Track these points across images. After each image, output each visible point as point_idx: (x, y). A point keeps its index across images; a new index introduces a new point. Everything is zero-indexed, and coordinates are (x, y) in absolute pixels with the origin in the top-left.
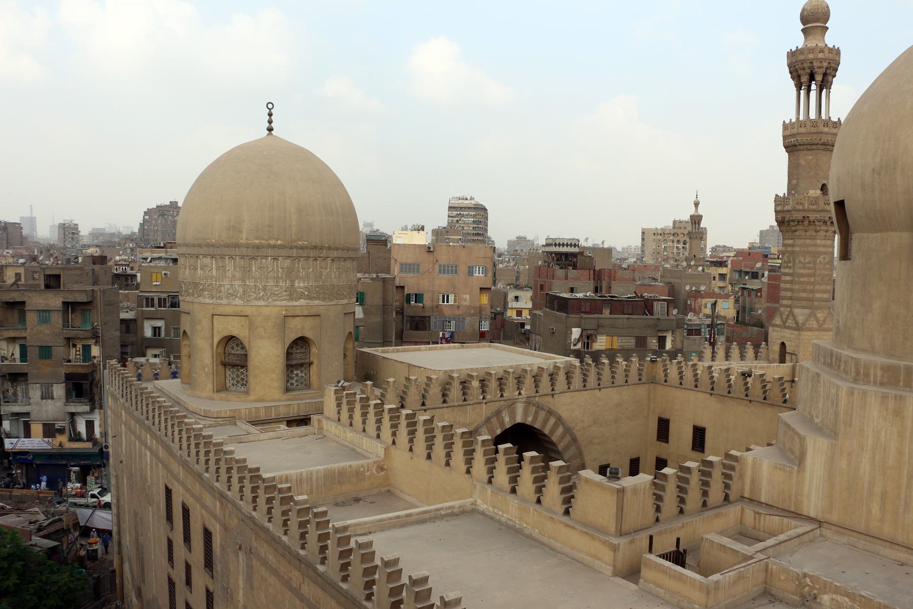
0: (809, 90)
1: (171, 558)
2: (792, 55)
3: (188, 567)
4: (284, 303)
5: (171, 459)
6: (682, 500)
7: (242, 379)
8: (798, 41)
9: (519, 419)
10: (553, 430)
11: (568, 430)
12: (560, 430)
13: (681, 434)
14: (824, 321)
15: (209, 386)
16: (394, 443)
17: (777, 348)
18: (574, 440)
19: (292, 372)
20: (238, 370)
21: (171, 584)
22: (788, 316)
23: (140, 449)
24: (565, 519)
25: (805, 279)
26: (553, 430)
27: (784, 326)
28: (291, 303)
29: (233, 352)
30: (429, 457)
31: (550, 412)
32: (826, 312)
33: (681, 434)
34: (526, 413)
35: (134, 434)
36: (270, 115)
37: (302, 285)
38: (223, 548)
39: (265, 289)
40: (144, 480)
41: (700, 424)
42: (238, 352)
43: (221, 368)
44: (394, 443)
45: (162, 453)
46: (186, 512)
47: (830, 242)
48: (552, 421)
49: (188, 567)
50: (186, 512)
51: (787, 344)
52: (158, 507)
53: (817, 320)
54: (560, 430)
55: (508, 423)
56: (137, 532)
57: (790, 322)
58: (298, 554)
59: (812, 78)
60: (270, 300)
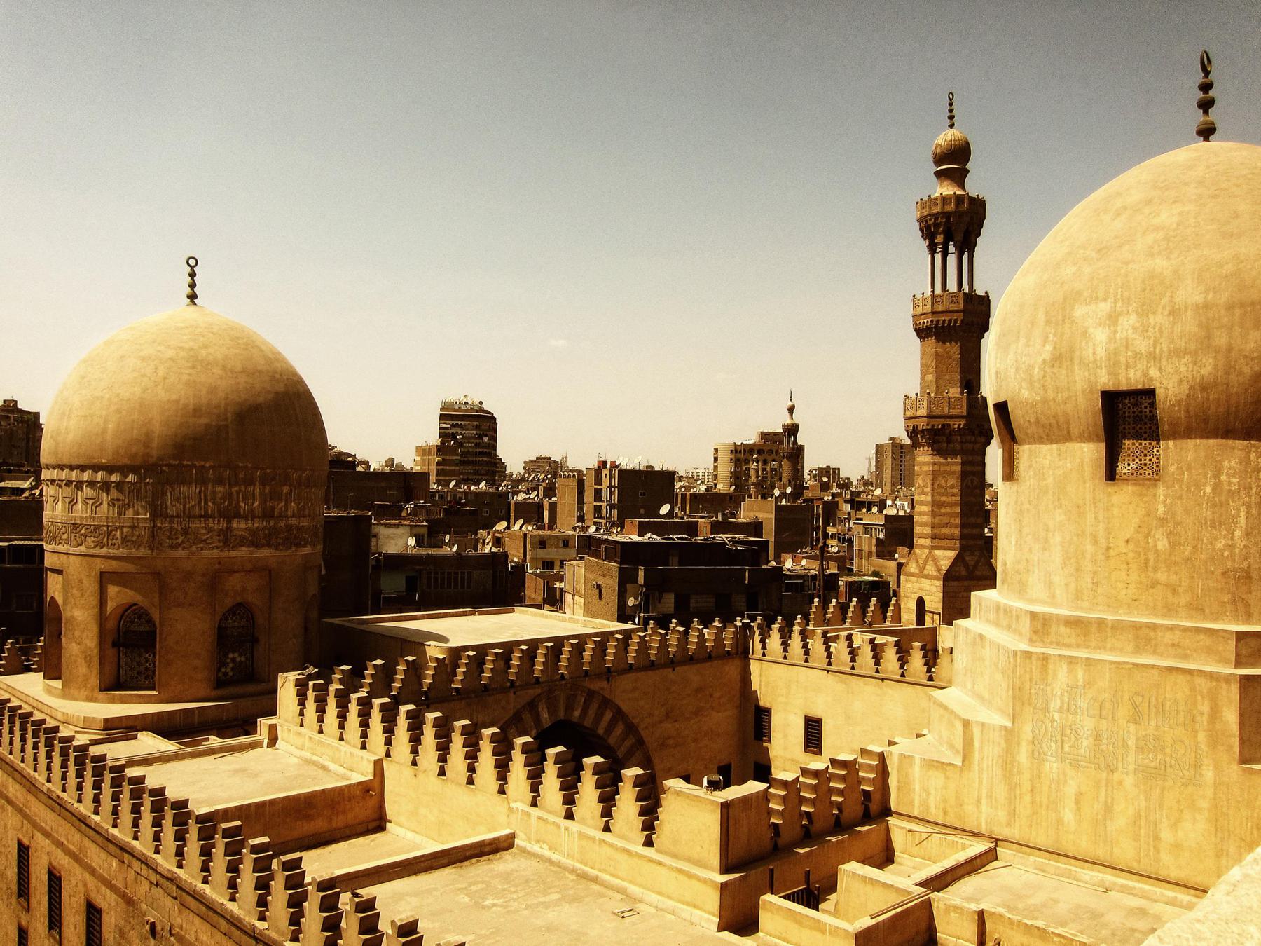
0: (945, 255)
4: (215, 554)
5: (30, 797)
7: (147, 669)
11: (631, 729)
12: (619, 729)
14: (975, 567)
15: (94, 680)
16: (388, 755)
17: (912, 605)
19: (226, 656)
20: (140, 656)
22: (926, 560)
24: (648, 851)
25: (948, 510)
26: (609, 730)
27: (921, 574)
28: (225, 555)
29: (132, 628)
30: (442, 773)
31: (606, 703)
32: (977, 553)
36: (193, 275)
37: (243, 526)
39: (185, 532)
41: (816, 712)
42: (142, 629)
43: (111, 652)
44: (388, 755)
46: (55, 881)
47: (979, 458)
48: (608, 716)
50: (55, 881)
51: (926, 598)
53: (966, 566)
58: (254, 928)
60: (194, 548)
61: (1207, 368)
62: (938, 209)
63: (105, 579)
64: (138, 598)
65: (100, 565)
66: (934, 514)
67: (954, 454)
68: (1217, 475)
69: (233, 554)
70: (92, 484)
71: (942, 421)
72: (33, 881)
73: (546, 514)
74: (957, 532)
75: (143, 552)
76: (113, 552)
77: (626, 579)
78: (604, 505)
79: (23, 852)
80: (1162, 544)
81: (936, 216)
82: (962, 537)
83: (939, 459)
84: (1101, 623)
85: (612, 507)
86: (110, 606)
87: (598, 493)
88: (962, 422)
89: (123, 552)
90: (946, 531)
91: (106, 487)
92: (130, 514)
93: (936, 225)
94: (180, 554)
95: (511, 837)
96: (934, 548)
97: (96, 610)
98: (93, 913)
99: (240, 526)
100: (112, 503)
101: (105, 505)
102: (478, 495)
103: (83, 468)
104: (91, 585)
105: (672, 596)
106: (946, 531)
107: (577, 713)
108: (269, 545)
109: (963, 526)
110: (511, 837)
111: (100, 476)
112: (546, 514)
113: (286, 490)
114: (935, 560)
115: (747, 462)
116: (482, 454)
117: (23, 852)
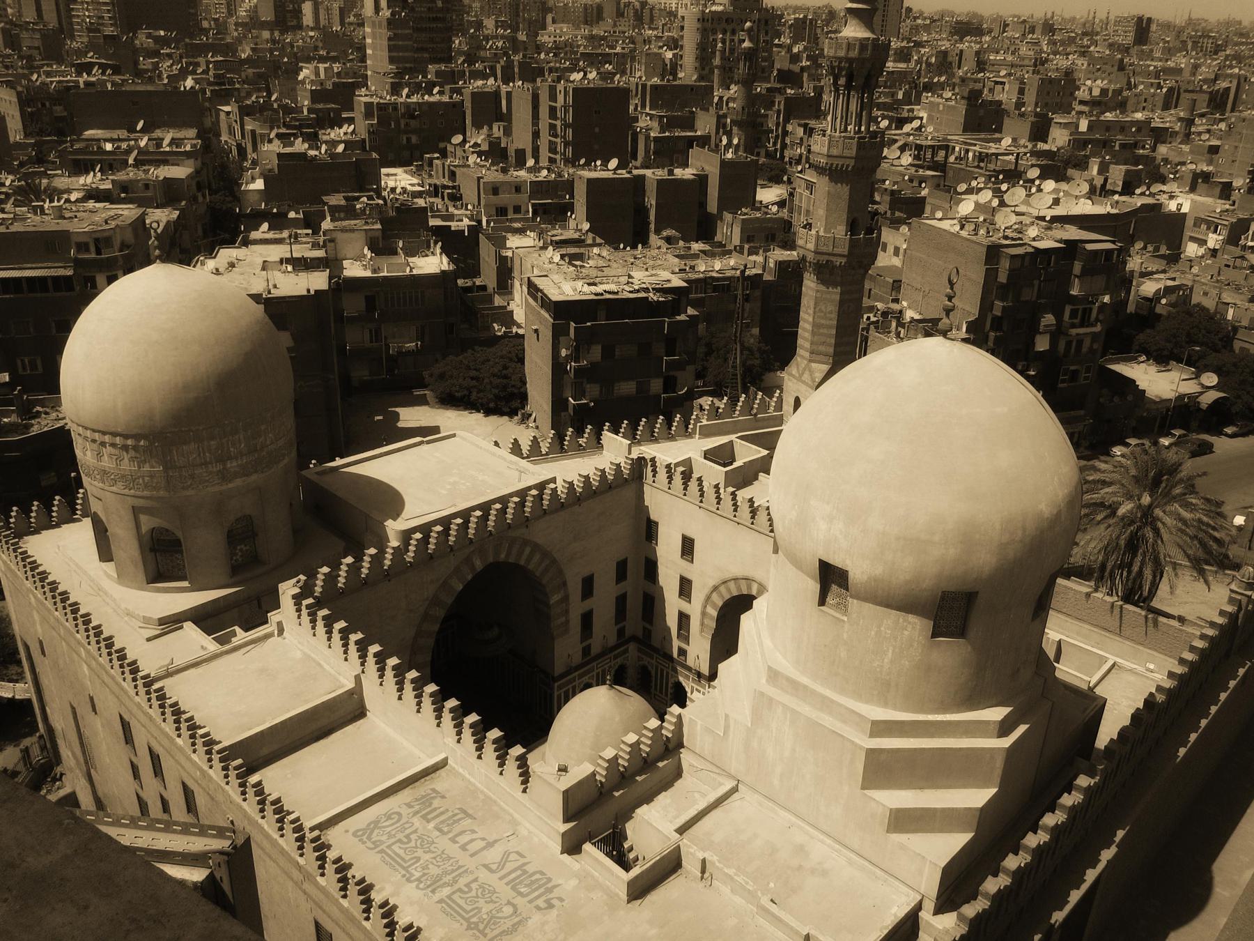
4: (217, 488)
9: (491, 560)
11: (546, 554)
12: (537, 557)
15: (141, 576)
18: (554, 561)
27: (799, 379)
28: (224, 487)
31: (526, 543)
37: (235, 464)
39: (192, 477)
48: (528, 550)
54: (537, 557)
55: (479, 564)
57: (806, 377)
61: (879, 570)
62: (842, 53)
63: (136, 511)
64: (165, 525)
65: (131, 501)
66: (813, 333)
67: (835, 285)
68: (879, 627)
69: (230, 485)
70: (113, 445)
71: (826, 257)
73: (504, 103)
74: (831, 350)
75: (162, 493)
76: (138, 493)
77: (558, 333)
78: (558, 123)
80: (843, 654)
81: (840, 59)
82: (836, 354)
83: (823, 288)
84: (805, 687)
85: (566, 126)
86: (144, 529)
87: (553, 111)
88: (844, 260)
89: (146, 493)
90: (822, 348)
91: (125, 448)
92: (147, 468)
93: (840, 69)
94: (190, 492)
95: (446, 759)
96: (810, 361)
97: (135, 531)
99: (232, 465)
100: (132, 459)
101: (126, 460)
102: (431, 105)
103: (104, 433)
104: (128, 517)
105: (599, 347)
106: (822, 348)
107: (503, 556)
108: (256, 472)
109: (836, 345)
110: (446, 759)
111: (118, 440)
112: (504, 103)
113: (263, 427)
114: (811, 372)
115: (714, 32)
116: (435, 19)
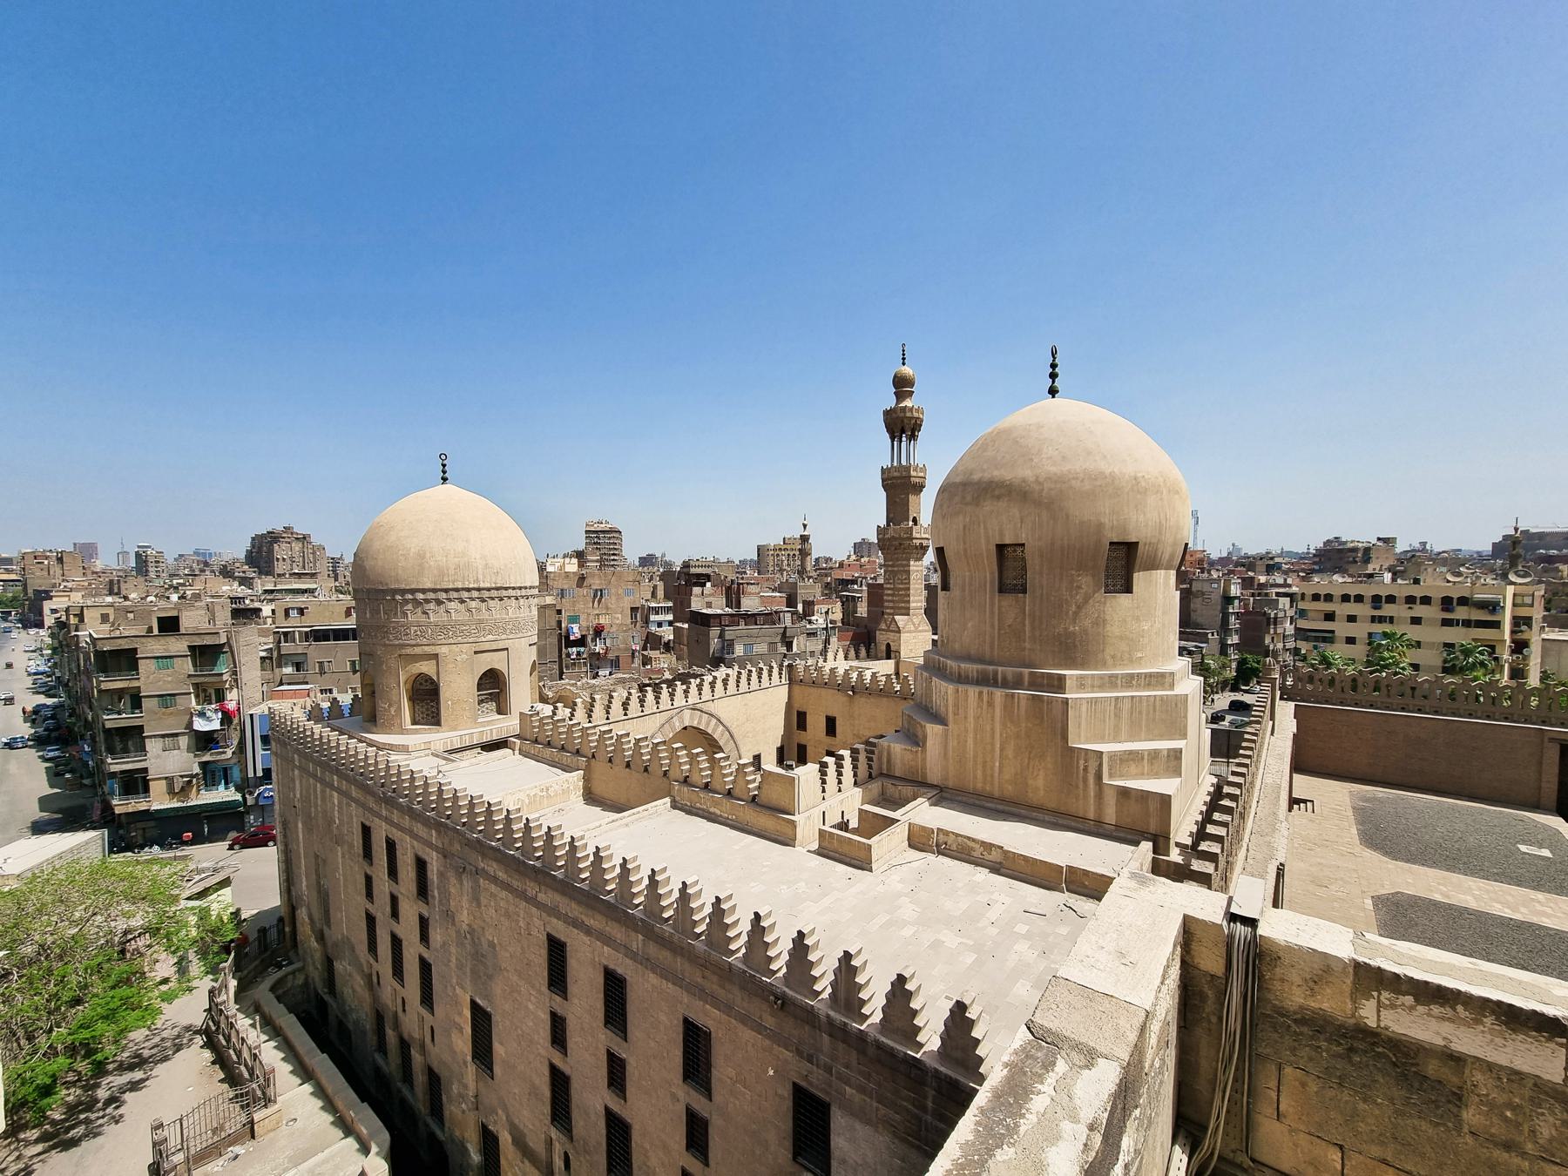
1: (369, 894)
2: (887, 413)
3: (394, 900)
6: (840, 782)
8: (891, 402)
10: (714, 730)
13: (816, 724)
21: (371, 920)
23: (323, 792)
26: (714, 730)
33: (816, 724)
34: (692, 718)
35: (315, 776)
38: (441, 875)
40: (330, 822)
45: (354, 792)
46: (391, 846)
49: (394, 900)
50: (391, 846)
52: (351, 846)
56: (318, 875)
57: (893, 627)
59: (903, 431)
72: (374, 847)
79: (366, 831)
98: (421, 865)
117: (366, 831)
